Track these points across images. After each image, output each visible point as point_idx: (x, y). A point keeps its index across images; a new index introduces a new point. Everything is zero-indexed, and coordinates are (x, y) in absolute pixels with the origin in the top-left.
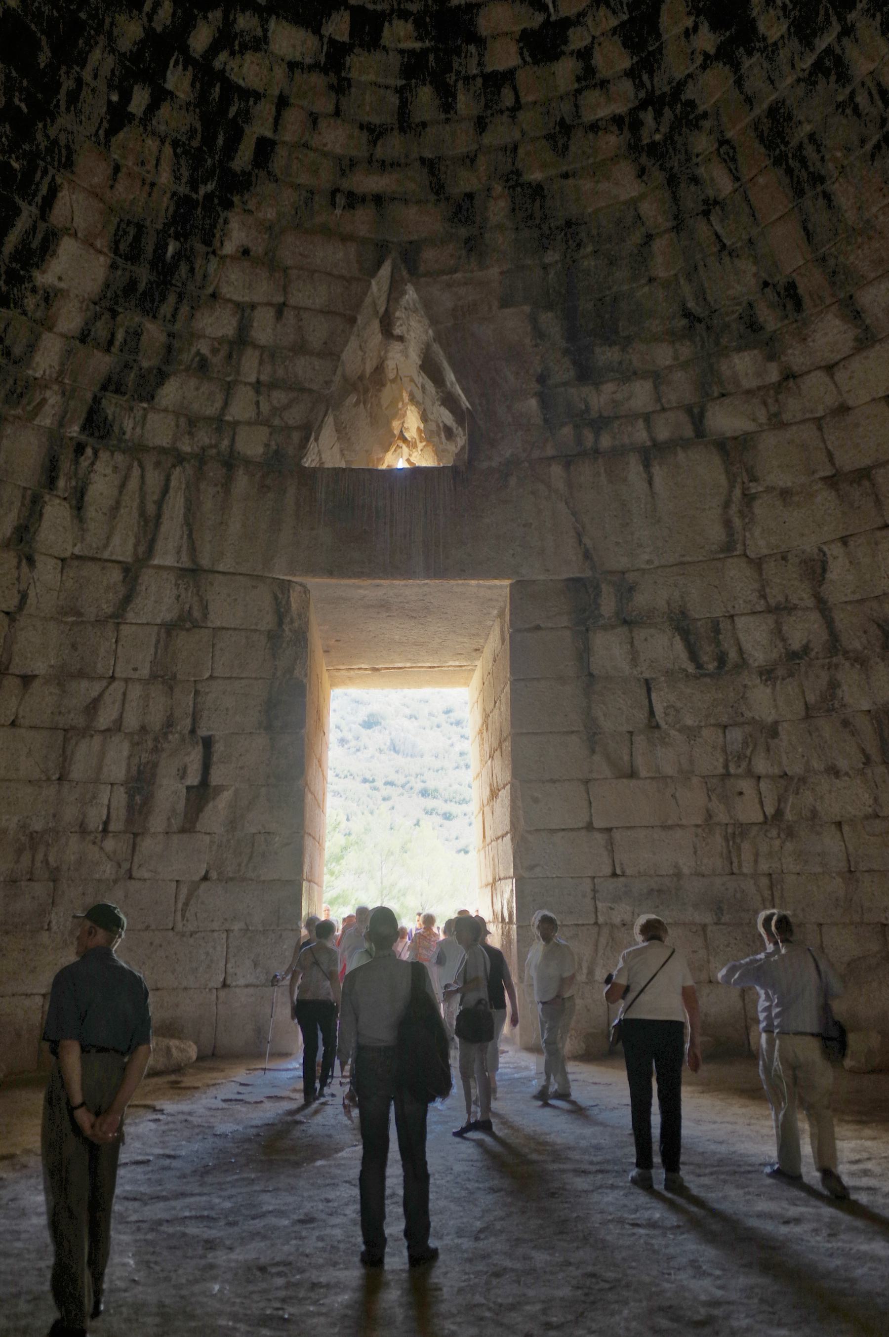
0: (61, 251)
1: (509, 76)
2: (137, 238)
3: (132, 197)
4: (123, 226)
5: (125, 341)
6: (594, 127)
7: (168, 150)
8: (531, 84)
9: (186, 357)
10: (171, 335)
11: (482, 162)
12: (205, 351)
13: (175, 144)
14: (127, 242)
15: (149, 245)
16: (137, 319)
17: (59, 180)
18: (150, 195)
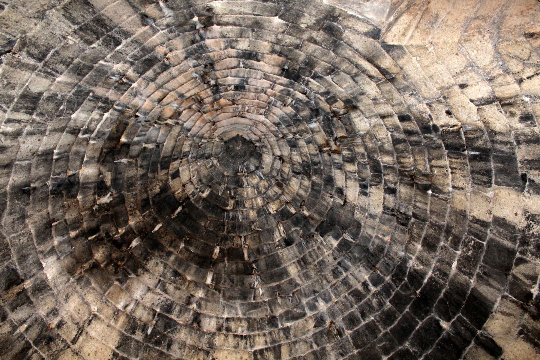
0: (502, 216)
1: (273, 52)
2: (478, 173)
3: (462, 178)
4: (476, 181)
5: (536, 169)
6: (234, 24)
7: (434, 162)
8: (264, 46)
9: (527, 130)
10: (519, 143)
11: (305, 36)
12: (516, 119)
13: (430, 161)
14: (483, 179)
15: (479, 165)
16: (519, 165)
17: (471, 218)
18: (456, 169)
